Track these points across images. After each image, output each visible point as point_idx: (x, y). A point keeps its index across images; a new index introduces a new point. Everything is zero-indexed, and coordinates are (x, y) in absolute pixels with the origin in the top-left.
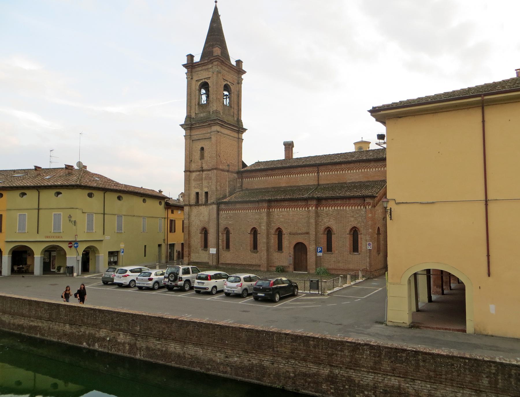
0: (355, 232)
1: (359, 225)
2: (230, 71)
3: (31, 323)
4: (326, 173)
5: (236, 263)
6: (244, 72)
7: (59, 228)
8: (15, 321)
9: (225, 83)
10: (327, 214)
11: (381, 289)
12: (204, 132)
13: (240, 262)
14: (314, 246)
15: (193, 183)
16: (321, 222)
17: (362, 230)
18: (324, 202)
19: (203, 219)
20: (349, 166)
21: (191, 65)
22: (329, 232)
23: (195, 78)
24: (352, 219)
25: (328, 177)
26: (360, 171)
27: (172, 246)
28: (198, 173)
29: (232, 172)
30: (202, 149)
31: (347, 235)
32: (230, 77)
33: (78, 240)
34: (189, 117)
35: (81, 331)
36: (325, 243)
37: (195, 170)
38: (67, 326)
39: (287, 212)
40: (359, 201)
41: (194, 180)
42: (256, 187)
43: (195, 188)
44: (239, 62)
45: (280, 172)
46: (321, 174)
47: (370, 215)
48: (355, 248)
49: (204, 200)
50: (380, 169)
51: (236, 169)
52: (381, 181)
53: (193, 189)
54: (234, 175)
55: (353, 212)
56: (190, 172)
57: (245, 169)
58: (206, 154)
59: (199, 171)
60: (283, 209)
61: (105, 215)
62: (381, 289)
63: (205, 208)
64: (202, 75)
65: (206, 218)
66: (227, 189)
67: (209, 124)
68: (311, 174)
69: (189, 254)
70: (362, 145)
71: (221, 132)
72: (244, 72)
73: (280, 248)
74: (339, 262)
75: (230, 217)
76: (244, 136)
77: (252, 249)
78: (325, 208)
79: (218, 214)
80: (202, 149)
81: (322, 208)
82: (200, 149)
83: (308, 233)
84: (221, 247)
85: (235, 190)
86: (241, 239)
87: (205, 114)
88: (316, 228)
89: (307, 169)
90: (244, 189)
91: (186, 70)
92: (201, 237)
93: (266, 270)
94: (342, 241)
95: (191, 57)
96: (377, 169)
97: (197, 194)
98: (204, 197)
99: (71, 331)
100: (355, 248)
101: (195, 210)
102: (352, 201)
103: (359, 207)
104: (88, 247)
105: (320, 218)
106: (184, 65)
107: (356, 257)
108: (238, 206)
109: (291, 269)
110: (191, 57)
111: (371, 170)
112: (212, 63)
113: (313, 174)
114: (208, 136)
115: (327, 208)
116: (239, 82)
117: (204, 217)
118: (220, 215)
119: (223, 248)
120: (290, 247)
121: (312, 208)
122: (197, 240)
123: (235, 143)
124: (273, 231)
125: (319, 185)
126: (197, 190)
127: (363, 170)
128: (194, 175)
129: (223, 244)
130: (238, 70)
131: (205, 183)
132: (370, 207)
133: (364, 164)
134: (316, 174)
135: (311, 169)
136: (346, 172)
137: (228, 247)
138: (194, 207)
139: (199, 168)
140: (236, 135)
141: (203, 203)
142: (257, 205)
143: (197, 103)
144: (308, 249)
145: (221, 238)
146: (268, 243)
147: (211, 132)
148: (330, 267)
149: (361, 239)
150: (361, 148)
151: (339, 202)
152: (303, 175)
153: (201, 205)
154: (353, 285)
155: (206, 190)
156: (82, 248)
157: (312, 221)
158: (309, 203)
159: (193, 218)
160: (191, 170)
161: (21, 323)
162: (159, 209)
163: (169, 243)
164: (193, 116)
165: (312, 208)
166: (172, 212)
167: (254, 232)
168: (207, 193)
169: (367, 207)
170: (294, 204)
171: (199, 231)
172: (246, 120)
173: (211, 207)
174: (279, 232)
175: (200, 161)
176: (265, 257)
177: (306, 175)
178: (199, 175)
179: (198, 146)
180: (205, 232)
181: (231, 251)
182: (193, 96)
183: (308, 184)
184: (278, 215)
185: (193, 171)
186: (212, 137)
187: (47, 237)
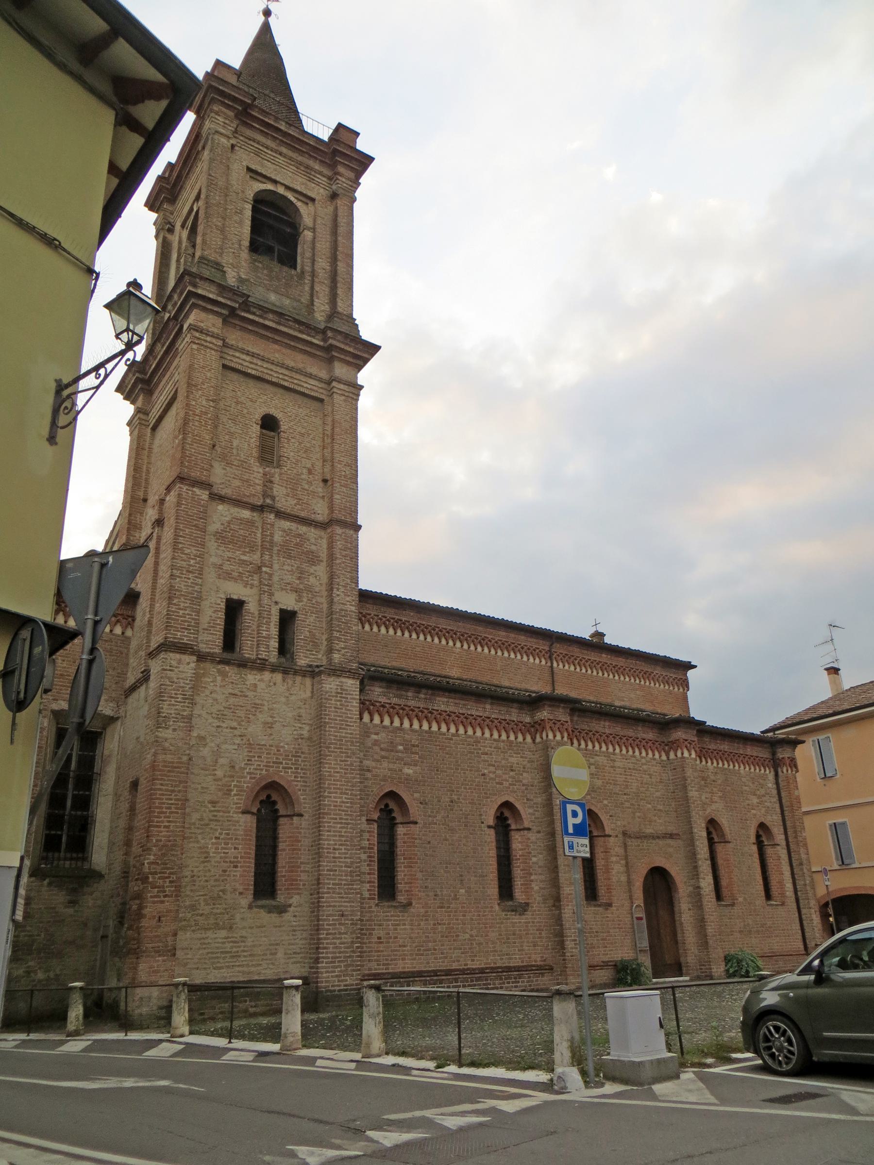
13: (457, 960)
19: (263, 740)
28: (246, 514)
39: (607, 755)
41: (220, 536)
43: (228, 576)
46: (555, 665)
53: (210, 576)
58: (289, 449)
63: (281, 688)
65: (286, 736)
75: (409, 748)
80: (269, 423)
82: (258, 416)
87: (287, 302)
97: (234, 609)
117: (269, 725)
122: (221, 847)
126: (237, 591)
128: (222, 513)
153: (261, 665)
155: (289, 602)
171: (236, 801)
173: (330, 684)
175: (257, 471)
178: (250, 523)
181: (417, 908)
185: (222, 499)
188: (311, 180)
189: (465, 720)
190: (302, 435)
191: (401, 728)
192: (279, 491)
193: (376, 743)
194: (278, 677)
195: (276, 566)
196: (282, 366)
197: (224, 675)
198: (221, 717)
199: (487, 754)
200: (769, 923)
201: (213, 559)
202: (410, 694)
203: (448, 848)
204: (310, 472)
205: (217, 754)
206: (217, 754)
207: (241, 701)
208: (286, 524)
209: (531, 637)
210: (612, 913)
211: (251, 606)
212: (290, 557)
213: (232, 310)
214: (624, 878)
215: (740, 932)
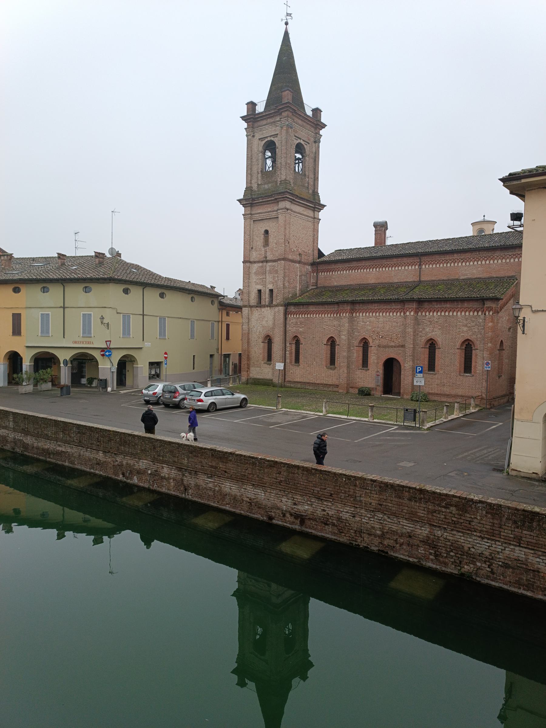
0: (468, 347)
2: (305, 124)
3: (58, 448)
4: (431, 266)
5: (308, 381)
6: (324, 126)
7: (90, 333)
8: (40, 444)
9: (298, 142)
10: (430, 321)
11: (501, 424)
12: (269, 210)
13: (312, 380)
14: (411, 363)
15: (254, 278)
16: (421, 332)
17: (478, 344)
18: (426, 305)
19: (266, 325)
20: (463, 256)
21: (252, 118)
22: (432, 345)
23: (258, 136)
24: (465, 329)
25: (433, 271)
26: (479, 263)
27: (227, 356)
28: (261, 264)
29: (305, 264)
30: (267, 232)
31: (457, 351)
32: (304, 133)
33: (111, 346)
34: (249, 190)
35: (117, 461)
36: (427, 359)
37: (257, 260)
38: (101, 454)
39: (376, 317)
40: (476, 305)
42: (335, 284)
43: (257, 284)
44: (317, 112)
45: (368, 263)
46: (424, 267)
47: (490, 324)
48: (467, 367)
49: (267, 300)
50: (508, 261)
51: (311, 260)
52: (508, 277)
56: (250, 262)
57: (322, 259)
59: (262, 262)
60: (371, 314)
61: (145, 316)
62: (501, 424)
64: (268, 131)
65: (270, 323)
66: (298, 285)
67: (276, 199)
68: (410, 267)
69: (248, 368)
70: (484, 226)
71: (291, 210)
72: (324, 126)
73: (365, 363)
74: (444, 385)
76: (322, 214)
77: (329, 365)
78: (427, 314)
79: (286, 319)
80: (267, 232)
81: (424, 314)
82: (263, 232)
83: (403, 346)
84: (288, 361)
85: (307, 287)
86: (314, 351)
87: (270, 185)
88: (414, 340)
89: (405, 260)
90: (319, 286)
91: (245, 125)
92: (264, 347)
93: (345, 392)
94: (449, 357)
95: (252, 105)
96: (504, 261)
97: (260, 291)
98: (267, 296)
99: (105, 460)
100: (467, 367)
101: (257, 313)
102: (466, 305)
103: (476, 313)
104: (124, 356)
106: (243, 118)
107: (467, 379)
108: (311, 308)
109: (378, 393)
110: (252, 105)
111: (496, 261)
112: (281, 114)
113: (413, 267)
114: (274, 214)
115: (431, 314)
116: (317, 141)
117: (267, 321)
118: (288, 319)
119: (291, 362)
120: (378, 363)
121: (410, 312)
122: (258, 350)
123: (310, 224)
124: (356, 342)
125: (420, 281)
126: (260, 287)
127: (484, 262)
128: (256, 266)
129: (291, 356)
130: (316, 122)
131: (269, 278)
132: (491, 313)
133: (485, 254)
134: (417, 267)
135: (410, 260)
136: (460, 264)
137: (297, 360)
138: (255, 309)
139: (262, 258)
140: (310, 213)
141: (267, 304)
142: (336, 308)
143: (260, 170)
144: (402, 367)
145: (288, 349)
146: (348, 357)
147: (278, 210)
148: (430, 391)
149: (476, 355)
150: (481, 231)
151: (448, 305)
152: (400, 268)
153: (264, 306)
154: (461, 417)
155: (270, 287)
156: (116, 357)
157: (410, 330)
158: (406, 306)
159: (253, 322)
160: (252, 260)
161: (46, 447)
162: (211, 311)
163: (223, 353)
164: (255, 187)
165: (410, 312)
166: (228, 314)
167: (332, 343)
168: (271, 291)
169: (487, 313)
170: (385, 307)
171: (261, 340)
173: (277, 309)
174: (365, 344)
176: (345, 375)
177: (403, 268)
178: (262, 266)
179: (262, 227)
180: (269, 340)
181: (301, 366)
182: (254, 160)
183: (405, 280)
184: (363, 322)
185: (255, 262)
186: (280, 216)
187: (76, 342)
188: (276, 126)
189: (319, 313)
190: (274, 232)
191: (299, 317)
192: (268, 254)
193: (292, 323)
194: (269, 308)
195: (268, 277)
196: (266, 212)
197: (257, 310)
198: (257, 320)
201: (255, 280)
203: (314, 351)
204: (276, 244)
205: (257, 329)
206: (257, 329)
207: (261, 316)
208: (270, 264)
211: (262, 291)
212: (271, 273)
213: (251, 204)
214: (375, 361)
215: (437, 385)
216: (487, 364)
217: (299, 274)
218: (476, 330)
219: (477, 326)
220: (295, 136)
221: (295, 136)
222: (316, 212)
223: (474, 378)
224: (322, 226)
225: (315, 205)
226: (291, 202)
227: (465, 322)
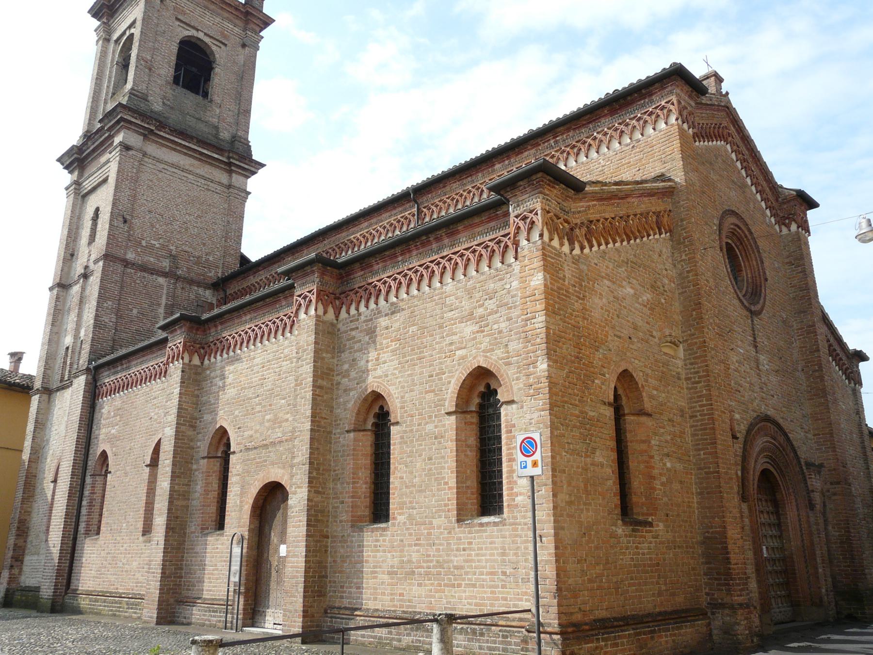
0: (481, 400)
1: (499, 353)
6: (267, 22)
22: (378, 417)
24: (468, 329)
51: (214, 274)
54: (201, 291)
55: (470, 293)
76: (253, 183)
78: (362, 308)
81: (353, 311)
105: (345, 356)
116: (251, 45)
124: (203, 446)
140: (222, 176)
172: (260, 141)
199: (155, 398)
200: (457, 560)
202: (119, 368)
209: (395, 208)
210: (222, 544)
216: (526, 453)
217: (164, 301)
218: (503, 325)
219: (503, 311)
220: (177, 19)
221: (177, 19)
222: (234, 175)
223: (507, 530)
224: (251, 207)
225: (229, 158)
226: (145, 136)
227: (466, 305)
